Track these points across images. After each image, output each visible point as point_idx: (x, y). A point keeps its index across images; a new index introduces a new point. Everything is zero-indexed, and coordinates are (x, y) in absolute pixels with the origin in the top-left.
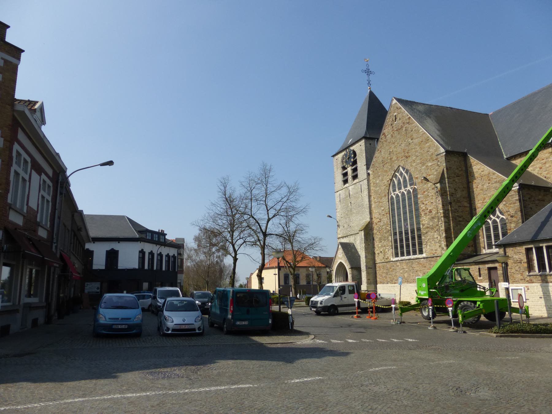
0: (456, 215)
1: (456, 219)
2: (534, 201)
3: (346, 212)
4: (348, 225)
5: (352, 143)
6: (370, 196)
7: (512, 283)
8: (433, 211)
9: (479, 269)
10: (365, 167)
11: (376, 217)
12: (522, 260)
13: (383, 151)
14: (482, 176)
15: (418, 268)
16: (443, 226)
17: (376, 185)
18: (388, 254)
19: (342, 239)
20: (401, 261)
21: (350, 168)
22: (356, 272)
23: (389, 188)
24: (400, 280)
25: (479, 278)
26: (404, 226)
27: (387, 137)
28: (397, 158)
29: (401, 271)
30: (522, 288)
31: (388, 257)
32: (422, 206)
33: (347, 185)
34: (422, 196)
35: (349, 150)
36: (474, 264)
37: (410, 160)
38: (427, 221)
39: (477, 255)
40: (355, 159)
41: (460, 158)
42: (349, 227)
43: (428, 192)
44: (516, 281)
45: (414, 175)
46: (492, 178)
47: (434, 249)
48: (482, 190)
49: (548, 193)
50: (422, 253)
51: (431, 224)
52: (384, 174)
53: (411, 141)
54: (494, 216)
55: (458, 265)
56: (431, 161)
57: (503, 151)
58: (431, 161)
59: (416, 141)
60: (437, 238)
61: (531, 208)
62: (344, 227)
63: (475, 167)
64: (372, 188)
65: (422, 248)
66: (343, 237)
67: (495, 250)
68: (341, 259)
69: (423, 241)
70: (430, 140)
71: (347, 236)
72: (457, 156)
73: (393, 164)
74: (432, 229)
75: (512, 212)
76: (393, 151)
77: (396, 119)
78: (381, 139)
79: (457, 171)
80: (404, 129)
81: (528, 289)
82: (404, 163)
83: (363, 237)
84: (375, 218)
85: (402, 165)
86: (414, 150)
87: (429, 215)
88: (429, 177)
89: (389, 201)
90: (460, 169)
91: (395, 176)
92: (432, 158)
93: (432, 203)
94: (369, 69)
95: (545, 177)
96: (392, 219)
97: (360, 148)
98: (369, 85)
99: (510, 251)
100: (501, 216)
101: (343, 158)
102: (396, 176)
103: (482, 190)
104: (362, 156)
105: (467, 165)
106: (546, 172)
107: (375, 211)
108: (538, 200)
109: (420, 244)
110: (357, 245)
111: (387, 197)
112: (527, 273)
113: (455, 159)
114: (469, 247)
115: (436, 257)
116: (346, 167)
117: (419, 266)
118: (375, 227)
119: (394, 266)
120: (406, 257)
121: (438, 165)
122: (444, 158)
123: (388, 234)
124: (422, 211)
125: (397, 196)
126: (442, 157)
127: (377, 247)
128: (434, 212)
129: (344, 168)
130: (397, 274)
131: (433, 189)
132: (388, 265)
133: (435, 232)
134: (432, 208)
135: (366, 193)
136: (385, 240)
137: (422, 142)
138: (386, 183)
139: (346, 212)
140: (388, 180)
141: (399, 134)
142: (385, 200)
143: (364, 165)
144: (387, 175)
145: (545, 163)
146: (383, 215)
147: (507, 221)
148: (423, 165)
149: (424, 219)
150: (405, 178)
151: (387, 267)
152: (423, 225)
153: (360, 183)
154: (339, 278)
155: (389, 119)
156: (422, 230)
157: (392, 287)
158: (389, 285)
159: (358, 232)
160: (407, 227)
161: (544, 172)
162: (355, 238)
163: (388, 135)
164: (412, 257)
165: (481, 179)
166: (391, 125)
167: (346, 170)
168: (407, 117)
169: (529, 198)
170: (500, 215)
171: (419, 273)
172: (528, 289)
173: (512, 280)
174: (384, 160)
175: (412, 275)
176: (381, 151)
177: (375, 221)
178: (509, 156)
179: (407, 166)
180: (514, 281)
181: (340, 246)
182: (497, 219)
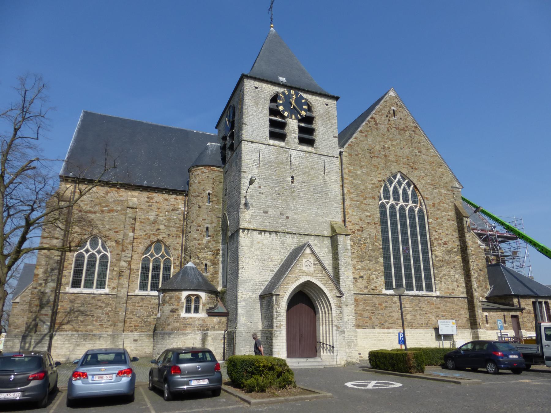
8: (448, 244)
9: (504, 316)
12: (531, 311)
15: (429, 309)
25: (505, 325)
43: (442, 221)
47: (450, 288)
60: (454, 276)
71: (276, 233)
74: (448, 264)
84: (350, 222)
87: (443, 247)
93: (447, 234)
115: (453, 297)
117: (431, 306)
119: (387, 302)
130: (393, 314)
132: (376, 300)
133: (452, 268)
136: (370, 261)
149: (437, 249)
151: (373, 303)
152: (436, 257)
157: (384, 333)
158: (377, 330)
171: (430, 315)
175: (418, 317)
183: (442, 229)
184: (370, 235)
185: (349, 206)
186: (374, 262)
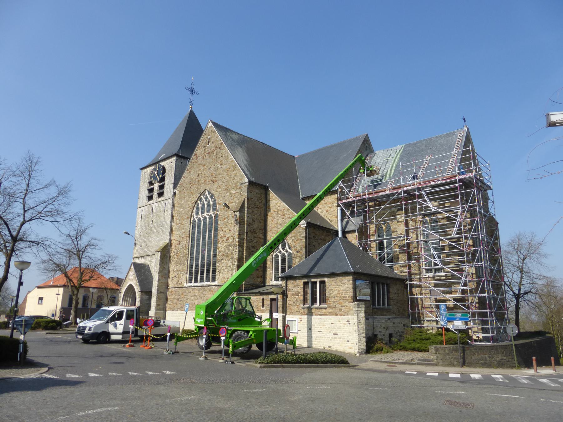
0: (251, 245)
1: (250, 249)
2: (317, 239)
3: (145, 230)
4: (146, 245)
5: (163, 159)
6: (172, 217)
7: (289, 315)
9: (263, 299)
10: (172, 186)
11: (176, 239)
12: (299, 293)
13: (192, 172)
14: (278, 211)
16: (237, 255)
17: (180, 205)
18: (182, 279)
19: (137, 259)
20: (194, 288)
21: (157, 184)
22: (145, 297)
23: (193, 210)
24: (186, 307)
25: (262, 308)
26: (202, 251)
27: (199, 158)
28: (205, 181)
29: (192, 298)
30: (297, 319)
31: (182, 282)
32: (220, 233)
33: (151, 202)
34: (222, 222)
35: (159, 165)
36: (259, 294)
37: (216, 185)
38: (223, 248)
39: (264, 286)
40: (163, 176)
41: (261, 190)
42: (147, 246)
43: (228, 220)
44: (292, 313)
45: (218, 201)
46: (286, 214)
47: (226, 277)
48: (276, 224)
49: (329, 234)
50: (215, 281)
51: (227, 251)
52: (190, 195)
53: (220, 167)
54: (284, 250)
55: (245, 295)
56: (235, 189)
57: (300, 191)
58: (235, 189)
59: (224, 167)
60: (230, 266)
61: (314, 246)
62: (141, 246)
63: (273, 201)
64: (176, 208)
65: (215, 275)
66: (138, 257)
67: (280, 282)
68: (131, 280)
69: (217, 268)
70: (237, 168)
71: (143, 256)
72: (259, 188)
73: (199, 187)
74: (227, 256)
75: (298, 247)
76: (201, 173)
77: (209, 141)
78: (193, 159)
79: (257, 202)
80: (215, 153)
81: (301, 321)
82: (210, 187)
83: (159, 259)
84: (174, 240)
85: (208, 189)
86: (221, 176)
88: (231, 204)
89: (190, 224)
90: (260, 201)
91: (199, 198)
92: (236, 186)
93: (230, 230)
94: (193, 88)
95: (330, 220)
96: (191, 243)
97: (170, 165)
98: (191, 104)
99: (291, 283)
100: (289, 251)
101: (152, 172)
102: (201, 200)
103: (276, 224)
104: (171, 173)
105: (267, 198)
106: (331, 215)
107: (175, 233)
108: (321, 239)
109: (214, 271)
110: (152, 267)
111: (189, 219)
112: (302, 306)
113: (257, 191)
114: (258, 277)
116: (153, 183)
118: (173, 249)
119: (186, 292)
120: (199, 284)
121: (241, 193)
122: (247, 188)
123: (185, 258)
124: (220, 237)
125: (199, 220)
126: (245, 186)
127: (172, 271)
128: (231, 240)
129: (151, 183)
130: (188, 301)
131: (233, 217)
132: (181, 291)
133: (230, 260)
134: (229, 236)
135: (169, 212)
136: (181, 264)
137: (229, 169)
138: (191, 205)
139: (145, 230)
140: (193, 202)
141: (210, 157)
142: (187, 222)
143: (172, 184)
144: (193, 196)
145: (331, 207)
146: (183, 237)
147: (293, 256)
148: (228, 191)
149: (221, 245)
150: (209, 202)
151: (179, 293)
152: (219, 252)
153: (165, 201)
154: (127, 302)
155: (203, 140)
156: (217, 256)
157: (181, 314)
159: (155, 253)
160: (204, 252)
161: (329, 216)
162: (151, 260)
163: (199, 157)
164: (205, 283)
165: (277, 213)
166: (204, 147)
167: (153, 186)
168: (220, 142)
169: (314, 237)
170: (288, 250)
172: (301, 321)
173: (289, 311)
174: (192, 181)
176: (190, 172)
177: (174, 243)
178: (304, 196)
179: (212, 191)
180: (291, 313)
181: (132, 267)
182: (285, 253)
183: (227, 227)
184: (183, 246)
185: (176, 229)
186: (183, 265)
